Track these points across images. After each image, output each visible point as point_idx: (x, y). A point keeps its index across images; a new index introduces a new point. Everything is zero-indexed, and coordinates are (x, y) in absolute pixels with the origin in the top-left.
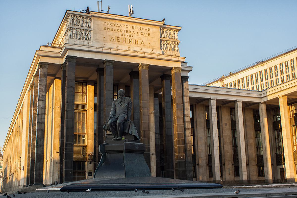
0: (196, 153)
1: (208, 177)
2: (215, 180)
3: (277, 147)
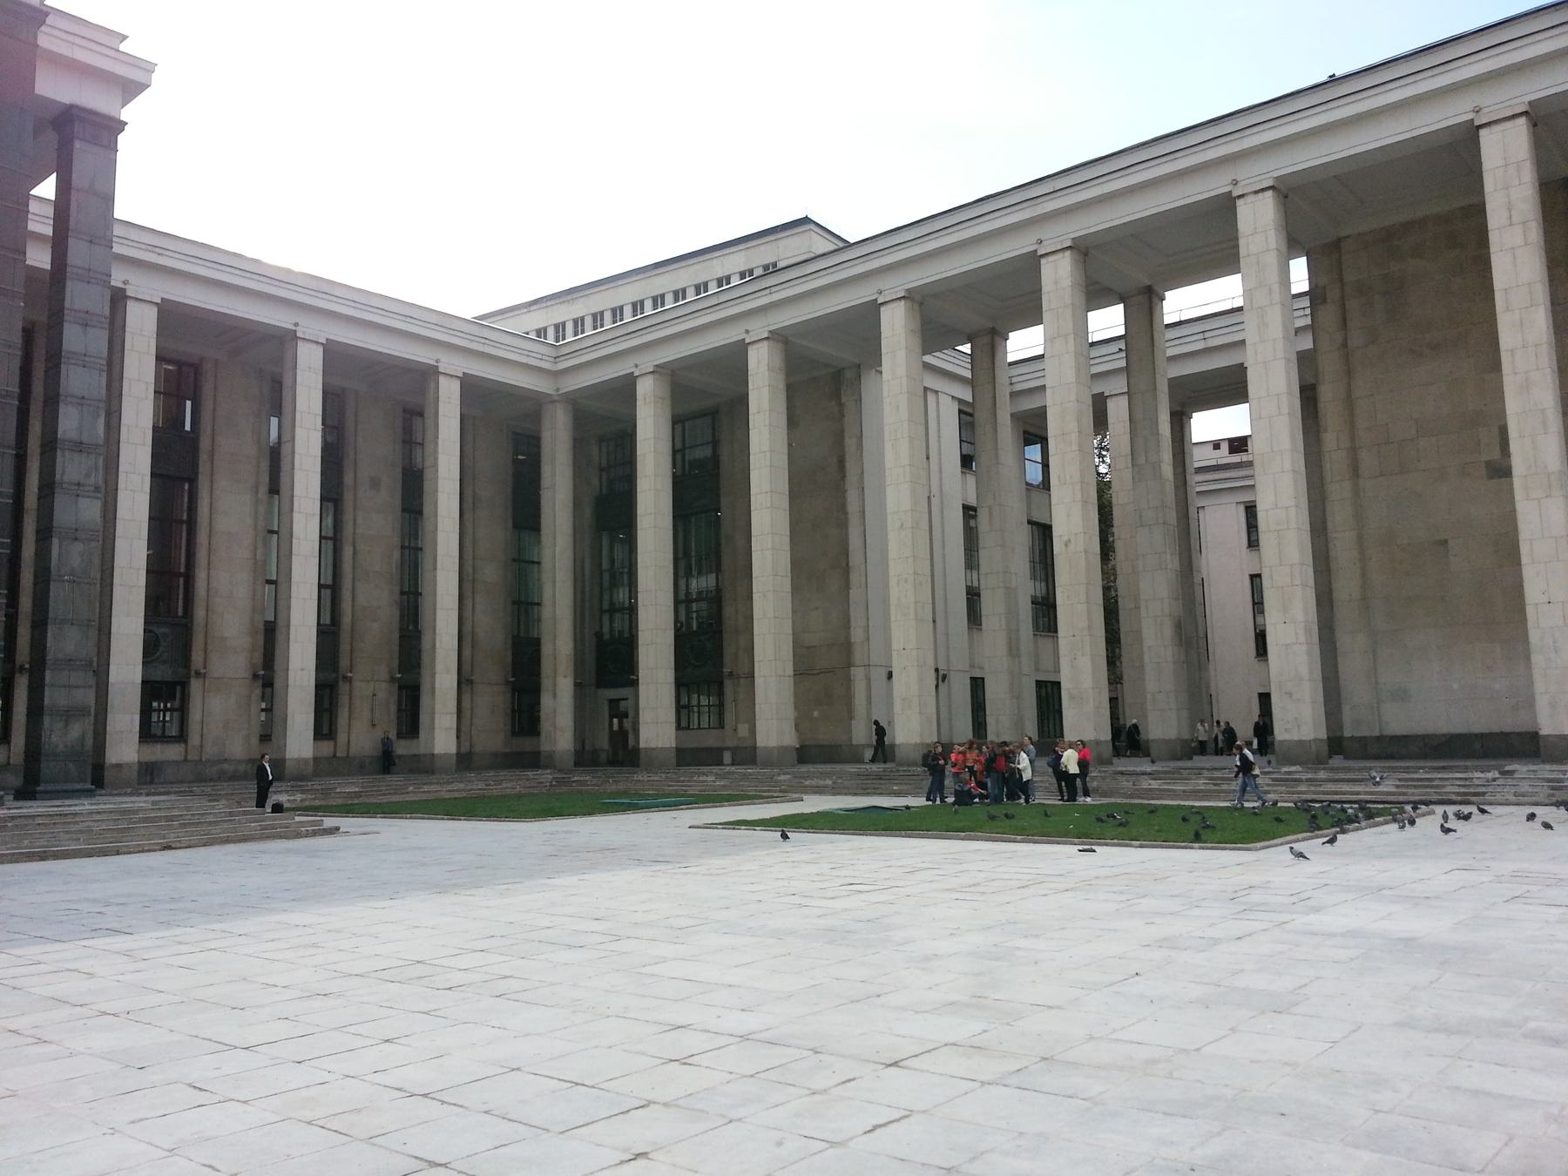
0: (199, 613)
1: (255, 740)
2: (284, 760)
3: (606, 606)
